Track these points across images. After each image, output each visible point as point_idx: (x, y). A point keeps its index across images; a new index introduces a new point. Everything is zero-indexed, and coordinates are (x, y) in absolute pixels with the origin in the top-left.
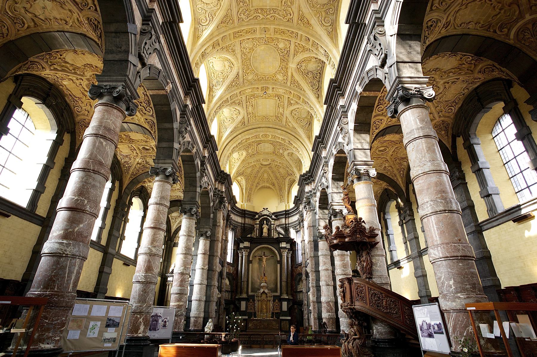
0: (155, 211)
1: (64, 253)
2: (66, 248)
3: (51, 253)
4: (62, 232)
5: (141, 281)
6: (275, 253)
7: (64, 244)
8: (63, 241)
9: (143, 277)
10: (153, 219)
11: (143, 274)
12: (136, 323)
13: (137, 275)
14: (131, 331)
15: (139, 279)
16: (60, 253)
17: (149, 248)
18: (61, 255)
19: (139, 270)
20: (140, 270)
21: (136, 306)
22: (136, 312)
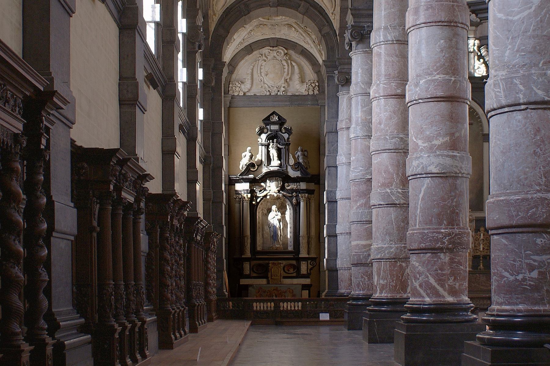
0: (397, 59)
1: (460, 172)
2: (461, 164)
3: (444, 173)
4: (447, 139)
5: (397, 202)
6: (477, 114)
7: (458, 158)
8: (453, 152)
9: (400, 195)
10: (398, 77)
11: (400, 190)
12: (402, 277)
13: (387, 192)
14: (396, 288)
15: (394, 198)
16: (456, 173)
17: (402, 138)
18: (457, 175)
19: (387, 181)
20: (390, 183)
21: (397, 248)
22: (399, 258)
